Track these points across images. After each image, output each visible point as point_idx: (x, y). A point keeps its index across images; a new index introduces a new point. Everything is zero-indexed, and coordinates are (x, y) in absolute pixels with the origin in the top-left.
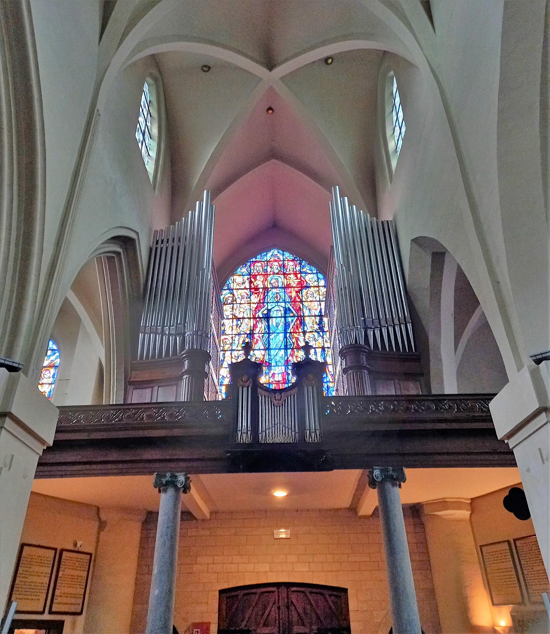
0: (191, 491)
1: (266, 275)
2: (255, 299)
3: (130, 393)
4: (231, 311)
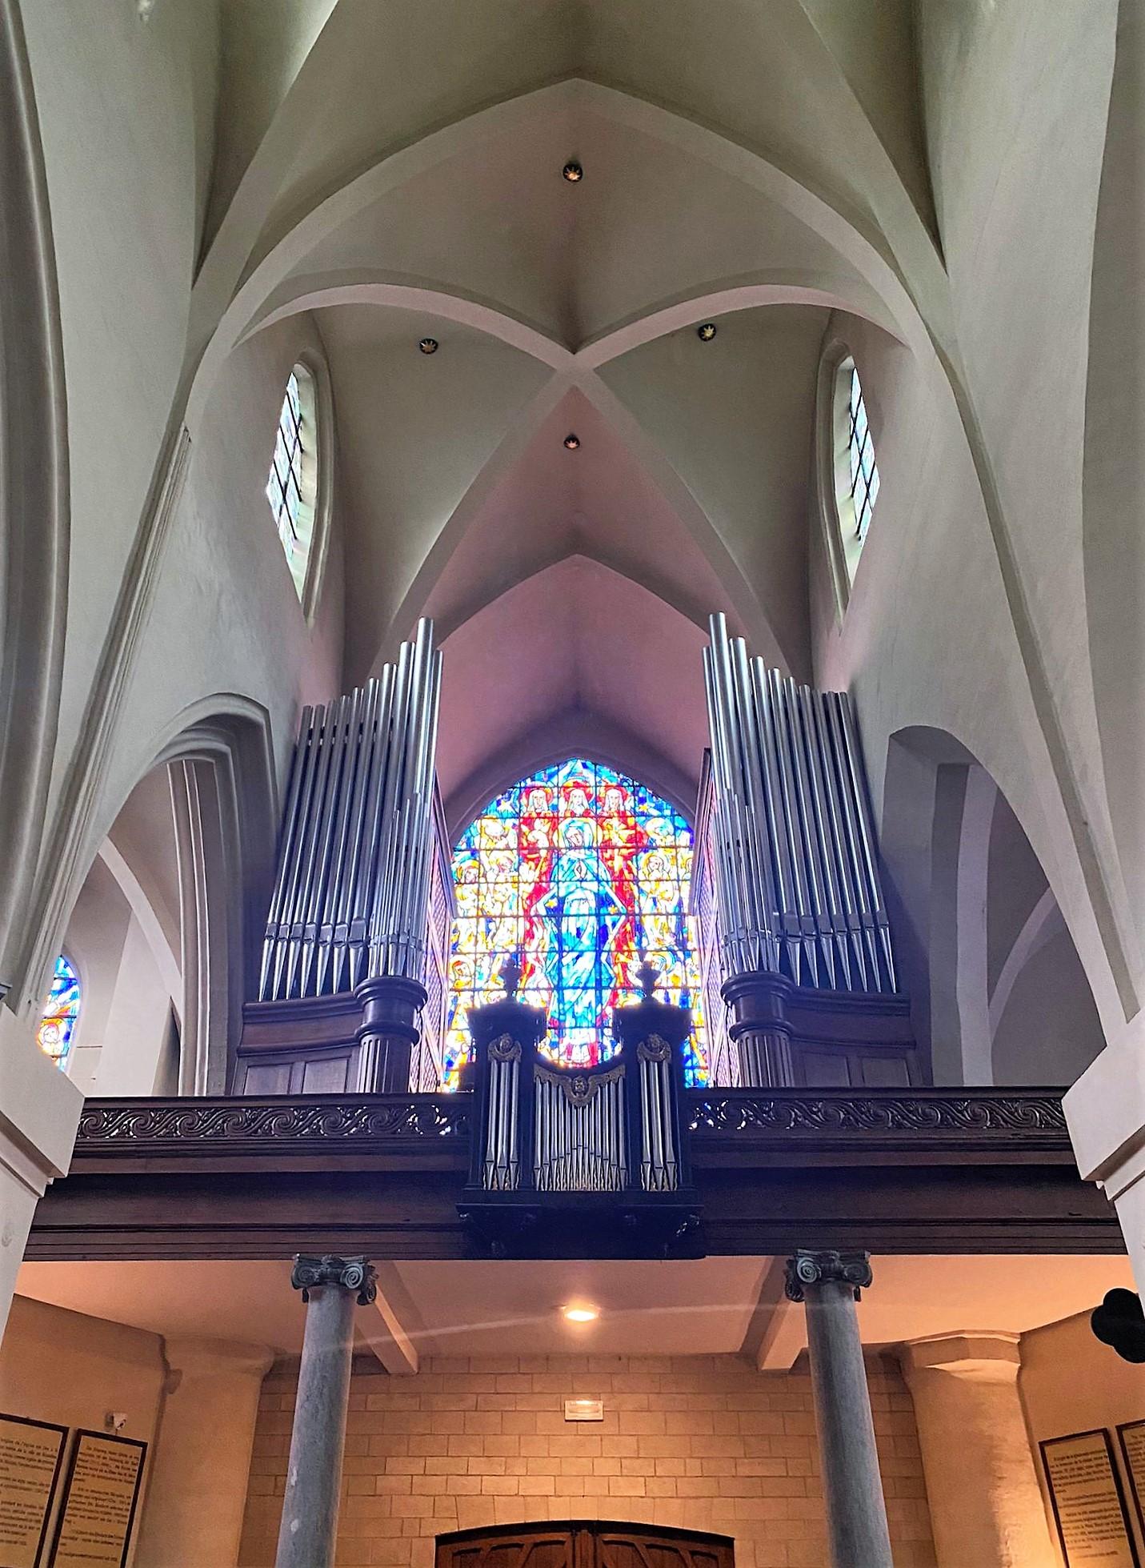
0: (376, 1302)
1: (554, 821)
2: (530, 874)
3: (242, 1078)
4: (474, 901)
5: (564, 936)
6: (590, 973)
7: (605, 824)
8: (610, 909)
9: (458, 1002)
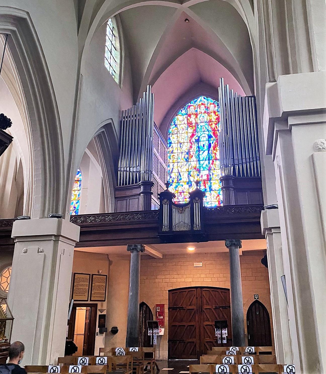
1: (196, 115)
2: (190, 130)
5: (200, 147)
7: (210, 115)
8: (211, 138)
9: (174, 166)
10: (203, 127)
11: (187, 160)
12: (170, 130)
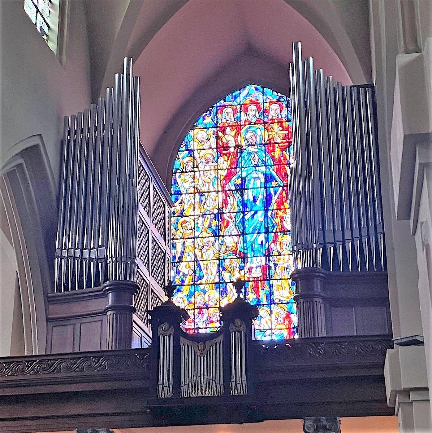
1: (238, 128)
2: (224, 163)
6: (262, 224)
8: (273, 183)
9: (186, 245)
10: (253, 156)
11: (216, 234)
12: (177, 164)
